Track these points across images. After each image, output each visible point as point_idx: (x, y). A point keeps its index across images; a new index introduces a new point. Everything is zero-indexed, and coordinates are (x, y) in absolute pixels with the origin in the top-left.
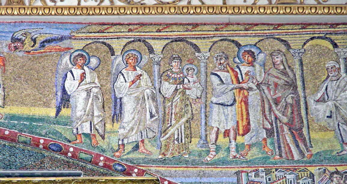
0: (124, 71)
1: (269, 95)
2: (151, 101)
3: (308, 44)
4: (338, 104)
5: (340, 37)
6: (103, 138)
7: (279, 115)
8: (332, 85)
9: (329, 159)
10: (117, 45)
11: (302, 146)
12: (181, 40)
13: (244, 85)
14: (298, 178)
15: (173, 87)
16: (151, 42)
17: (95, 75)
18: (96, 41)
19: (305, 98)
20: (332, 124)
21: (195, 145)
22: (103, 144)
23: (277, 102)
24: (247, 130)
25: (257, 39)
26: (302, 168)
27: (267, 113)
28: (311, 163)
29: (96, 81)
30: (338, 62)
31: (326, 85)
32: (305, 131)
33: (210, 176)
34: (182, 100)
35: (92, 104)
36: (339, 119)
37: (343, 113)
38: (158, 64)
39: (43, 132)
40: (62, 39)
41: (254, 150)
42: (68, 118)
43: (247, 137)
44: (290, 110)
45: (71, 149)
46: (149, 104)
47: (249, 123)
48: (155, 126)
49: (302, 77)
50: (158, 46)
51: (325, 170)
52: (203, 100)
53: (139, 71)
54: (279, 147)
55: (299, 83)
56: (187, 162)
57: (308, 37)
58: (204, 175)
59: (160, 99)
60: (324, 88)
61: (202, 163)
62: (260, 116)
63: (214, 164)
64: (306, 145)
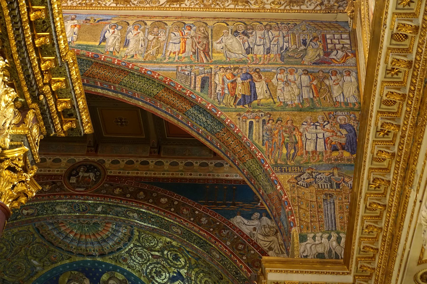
0: (132, 31)
1: (196, 40)
2: (142, 41)
6: (118, 53)
7: (199, 47)
8: (224, 39)
10: (131, 23)
11: (208, 58)
12: (160, 21)
13: (185, 37)
14: (204, 69)
15: (154, 37)
16: (146, 22)
17: (119, 32)
18: (122, 21)
19: (212, 42)
21: (159, 56)
22: (118, 55)
23: (199, 43)
24: (184, 52)
25: (193, 22)
27: (194, 46)
28: (211, 64)
29: (119, 34)
30: (229, 31)
32: (210, 53)
33: (164, 67)
34: (156, 41)
35: (116, 41)
38: (148, 29)
39: (92, 50)
40: (107, 20)
41: (186, 59)
42: (104, 46)
43: (183, 54)
44: (204, 46)
45: (103, 57)
46: (142, 42)
47: (185, 50)
48: (143, 50)
50: (149, 23)
52: (166, 41)
53: (139, 31)
54: (198, 58)
55: (210, 37)
56: (155, 62)
57: (216, 22)
58: (162, 67)
59: (146, 41)
61: (162, 63)
62: (190, 47)
63: (167, 63)
64: (210, 58)
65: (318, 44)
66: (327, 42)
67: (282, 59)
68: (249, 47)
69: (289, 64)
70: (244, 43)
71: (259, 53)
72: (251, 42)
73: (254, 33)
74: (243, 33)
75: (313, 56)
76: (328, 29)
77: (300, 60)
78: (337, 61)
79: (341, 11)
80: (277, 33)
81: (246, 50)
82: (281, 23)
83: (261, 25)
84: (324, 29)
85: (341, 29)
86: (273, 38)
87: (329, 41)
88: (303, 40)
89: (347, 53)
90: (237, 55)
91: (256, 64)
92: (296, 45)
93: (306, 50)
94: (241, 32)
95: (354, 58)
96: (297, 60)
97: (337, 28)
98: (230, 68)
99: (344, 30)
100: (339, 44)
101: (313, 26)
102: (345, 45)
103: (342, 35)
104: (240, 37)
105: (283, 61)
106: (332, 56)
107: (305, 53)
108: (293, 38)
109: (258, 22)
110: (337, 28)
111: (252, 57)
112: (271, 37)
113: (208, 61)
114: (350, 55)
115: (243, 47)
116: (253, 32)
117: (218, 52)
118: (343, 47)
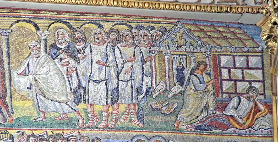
3: (14, 26)
4: (37, 78)
5: (42, 21)
8: (33, 62)
9: (27, 124)
19: (10, 71)
20: (31, 94)
26: (4, 130)
28: (12, 127)
31: (28, 61)
32: (8, 99)
36: (37, 90)
37: (41, 86)
49: (8, 53)
51: (23, 133)
57: (14, 20)
60: (26, 64)
64: (8, 111)
65: (206, 80)
66: (221, 75)
67: (140, 118)
68: (80, 86)
69: (151, 130)
70: (69, 76)
71: (97, 102)
72: (83, 74)
73: (87, 50)
74: (68, 48)
75: (196, 109)
76: (223, 43)
77: (173, 118)
78: (238, 123)
79: (250, 10)
80: (128, 52)
81: (74, 92)
82: (136, 28)
83: (99, 30)
84: (216, 41)
85: (248, 43)
86: (123, 64)
87: (225, 73)
88: (177, 69)
89: (256, 104)
90: (57, 104)
91: (93, 128)
92: (165, 82)
93: (182, 93)
94: (63, 47)
95: (269, 115)
96: (168, 119)
97: (239, 39)
98: (46, 137)
99: (253, 45)
100: (243, 80)
101: (197, 34)
102: (254, 84)
103: (250, 58)
104: (61, 59)
105: (142, 122)
106: (230, 111)
107: (181, 101)
108: (160, 65)
109: (94, 23)
110: (239, 39)
111: (87, 112)
112: (120, 62)
113: (5, 120)
114: (262, 107)
115: (68, 86)
116: (85, 47)
117: (24, 98)
118: (251, 88)
